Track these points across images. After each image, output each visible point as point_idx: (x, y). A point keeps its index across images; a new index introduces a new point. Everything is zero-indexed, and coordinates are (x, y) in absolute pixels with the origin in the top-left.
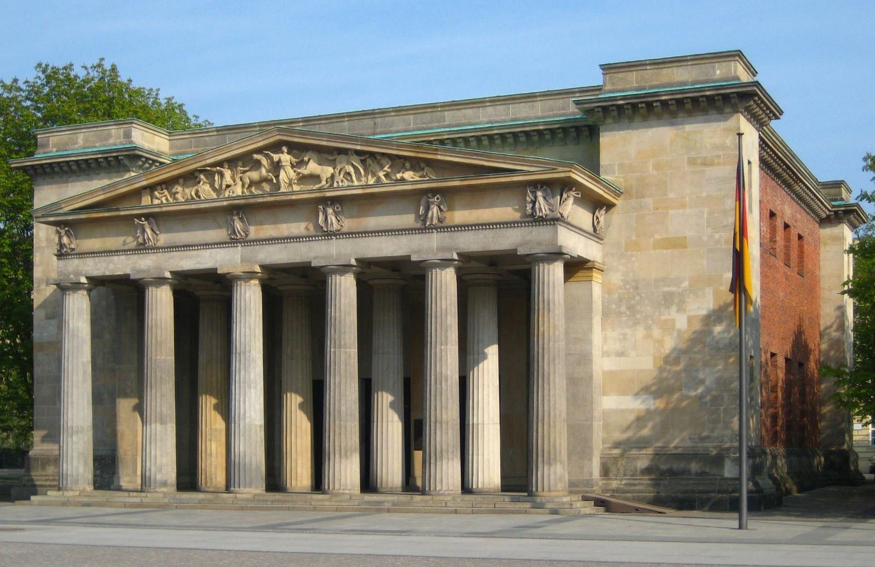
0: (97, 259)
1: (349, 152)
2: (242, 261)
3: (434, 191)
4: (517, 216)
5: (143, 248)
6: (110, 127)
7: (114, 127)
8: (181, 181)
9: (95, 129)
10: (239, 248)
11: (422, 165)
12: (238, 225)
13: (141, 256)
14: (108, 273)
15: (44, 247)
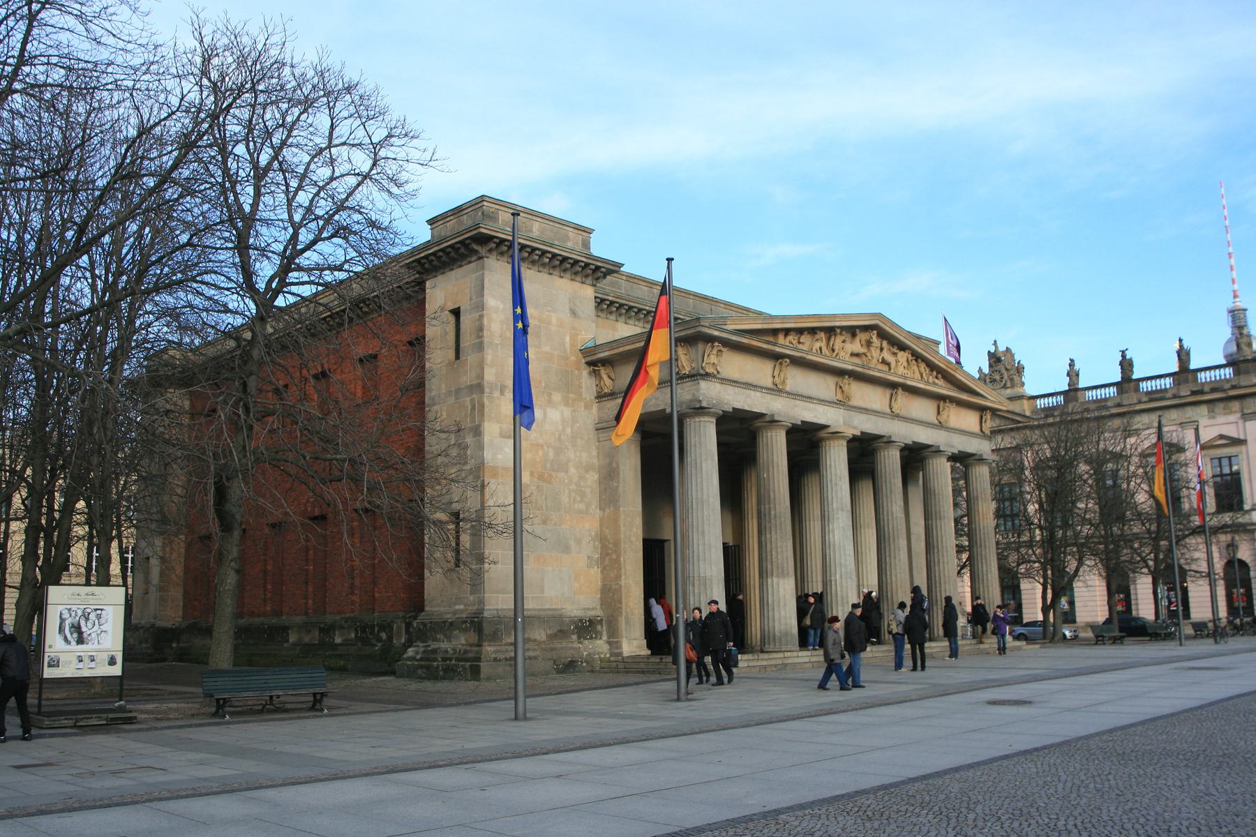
0: (737, 389)
1: (907, 351)
2: (844, 424)
3: (952, 400)
4: (976, 429)
5: (776, 390)
6: (568, 228)
7: (571, 230)
8: (806, 333)
9: (551, 224)
10: (842, 410)
11: (940, 376)
12: (846, 388)
13: (773, 396)
14: (746, 408)
15: (497, 345)
